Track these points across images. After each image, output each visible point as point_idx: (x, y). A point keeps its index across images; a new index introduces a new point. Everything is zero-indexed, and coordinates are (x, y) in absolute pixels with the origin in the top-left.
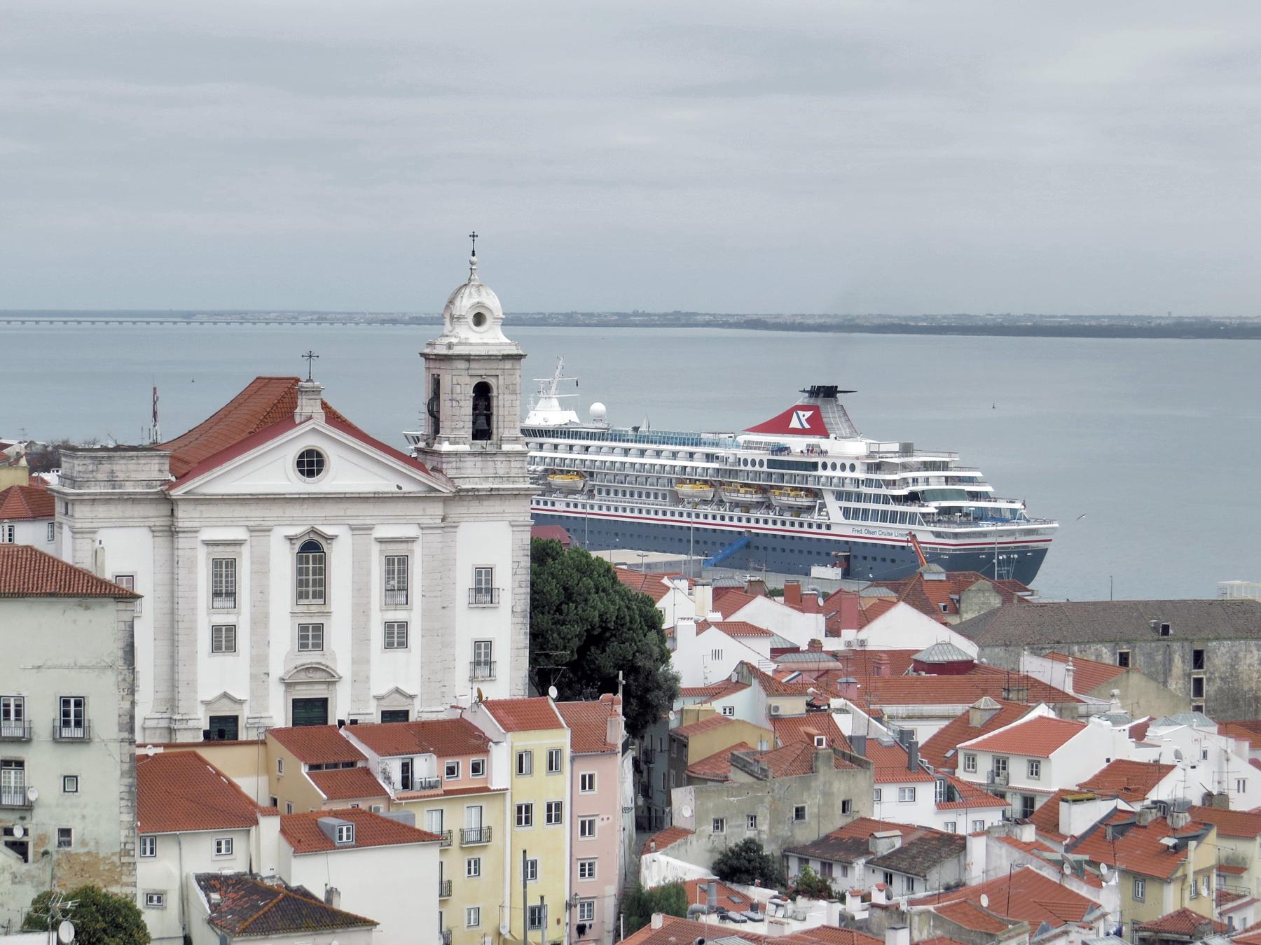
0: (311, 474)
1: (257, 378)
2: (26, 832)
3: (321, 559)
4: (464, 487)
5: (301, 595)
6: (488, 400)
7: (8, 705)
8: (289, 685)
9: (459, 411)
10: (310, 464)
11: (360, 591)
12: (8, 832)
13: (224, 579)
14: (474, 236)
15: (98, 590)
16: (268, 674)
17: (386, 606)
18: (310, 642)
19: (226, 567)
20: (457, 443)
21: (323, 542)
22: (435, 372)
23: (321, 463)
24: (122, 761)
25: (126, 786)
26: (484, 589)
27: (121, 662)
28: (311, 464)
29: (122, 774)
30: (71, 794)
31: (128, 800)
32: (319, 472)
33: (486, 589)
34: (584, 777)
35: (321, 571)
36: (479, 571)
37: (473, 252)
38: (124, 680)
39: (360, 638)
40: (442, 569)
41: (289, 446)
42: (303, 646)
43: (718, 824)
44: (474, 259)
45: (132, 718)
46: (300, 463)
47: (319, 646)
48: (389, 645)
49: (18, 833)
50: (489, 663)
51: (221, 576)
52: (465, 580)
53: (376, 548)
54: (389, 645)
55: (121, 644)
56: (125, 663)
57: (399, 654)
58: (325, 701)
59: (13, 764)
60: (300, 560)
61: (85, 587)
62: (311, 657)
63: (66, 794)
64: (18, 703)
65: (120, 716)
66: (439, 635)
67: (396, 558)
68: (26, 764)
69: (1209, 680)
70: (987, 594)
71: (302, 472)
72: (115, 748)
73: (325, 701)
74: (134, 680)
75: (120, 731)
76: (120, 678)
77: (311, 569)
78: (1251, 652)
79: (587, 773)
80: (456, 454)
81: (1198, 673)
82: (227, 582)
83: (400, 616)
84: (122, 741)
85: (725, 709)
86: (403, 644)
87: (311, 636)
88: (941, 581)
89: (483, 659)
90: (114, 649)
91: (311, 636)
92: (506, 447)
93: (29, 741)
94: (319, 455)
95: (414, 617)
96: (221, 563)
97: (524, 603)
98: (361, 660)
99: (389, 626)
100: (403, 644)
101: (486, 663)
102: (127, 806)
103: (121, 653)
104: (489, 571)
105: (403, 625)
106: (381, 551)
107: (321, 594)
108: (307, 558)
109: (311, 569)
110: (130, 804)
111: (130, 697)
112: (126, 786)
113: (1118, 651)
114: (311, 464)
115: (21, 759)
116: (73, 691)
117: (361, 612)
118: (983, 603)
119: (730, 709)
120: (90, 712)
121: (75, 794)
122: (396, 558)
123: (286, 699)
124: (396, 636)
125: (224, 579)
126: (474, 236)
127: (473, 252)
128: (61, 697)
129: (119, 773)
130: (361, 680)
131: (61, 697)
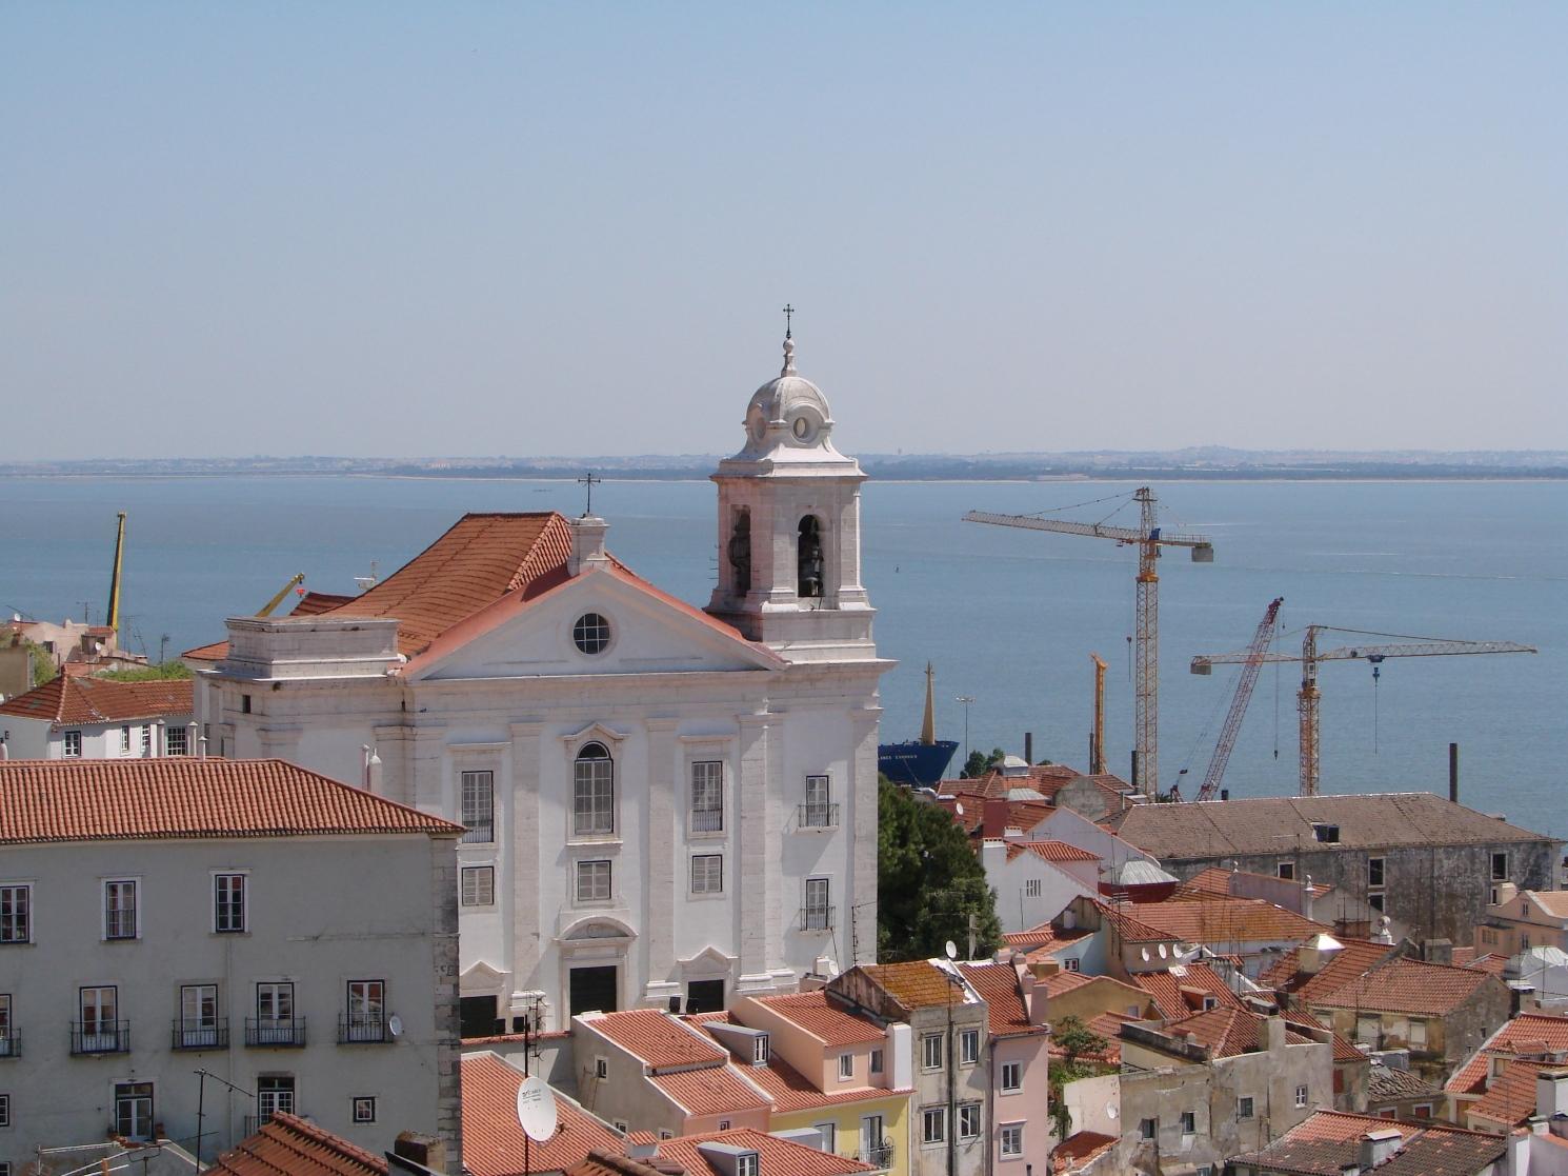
0: (592, 648)
1: (465, 517)
3: (608, 770)
4: (795, 662)
6: (816, 540)
7: (268, 996)
8: (566, 953)
9: (783, 553)
13: (477, 801)
14: (789, 310)
15: (403, 823)
16: (538, 935)
18: (594, 887)
19: (481, 784)
20: (780, 602)
21: (607, 742)
22: (740, 503)
23: (605, 633)
24: (440, 1074)
25: (447, 1109)
27: (439, 928)
28: (591, 634)
29: (442, 1095)
30: (365, 1124)
31: (450, 1130)
32: (603, 645)
33: (822, 806)
34: (1006, 1068)
37: (788, 332)
38: (444, 954)
42: (584, 894)
43: (1150, 1127)
44: (790, 341)
46: (578, 634)
47: (606, 891)
50: (825, 910)
51: (473, 798)
54: (697, 887)
55: (439, 901)
56: (444, 929)
58: (613, 970)
59: (276, 1081)
60: (580, 771)
61: (382, 819)
62: (595, 913)
63: (357, 1124)
64: (283, 992)
65: (437, 1007)
67: (707, 765)
68: (296, 1082)
69: (1389, 897)
70: (1088, 793)
71: (580, 646)
73: (613, 970)
74: (458, 953)
75: (438, 1028)
76: (439, 950)
77: (593, 782)
78: (1440, 861)
79: (1010, 1064)
80: (781, 616)
81: (1376, 890)
82: (481, 805)
84: (442, 1042)
85: (1067, 963)
87: (595, 875)
88: (1024, 778)
89: (817, 905)
91: (595, 875)
92: (845, 606)
93: (303, 1045)
94: (602, 621)
95: (728, 850)
96: (473, 777)
101: (821, 910)
102: (449, 1139)
103: (438, 914)
106: (687, 755)
108: (589, 767)
109: (593, 782)
110: (453, 1137)
111: (452, 979)
112: (447, 1109)
113: (1279, 864)
114: (591, 634)
115: (289, 1075)
116: (365, 971)
118: (1083, 806)
119: (1074, 963)
120: (394, 999)
121: (372, 1124)
122: (707, 765)
123: (561, 969)
124: (707, 875)
125: (477, 801)
126: (789, 310)
127: (788, 332)
128: (349, 982)
129: (436, 1093)
131: (349, 982)
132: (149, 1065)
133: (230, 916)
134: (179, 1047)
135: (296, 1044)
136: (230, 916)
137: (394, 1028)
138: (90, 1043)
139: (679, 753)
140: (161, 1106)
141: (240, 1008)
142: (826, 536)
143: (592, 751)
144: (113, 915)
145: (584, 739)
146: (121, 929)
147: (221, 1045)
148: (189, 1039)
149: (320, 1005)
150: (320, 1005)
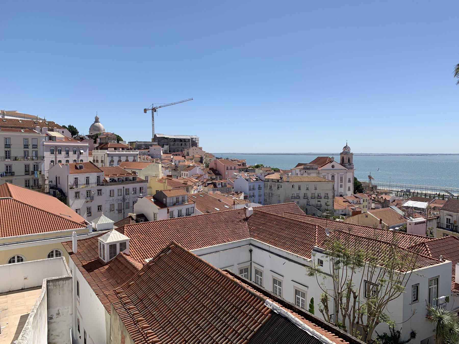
0: (333, 168)
10: (333, 167)
11: (338, 181)
17: (341, 183)
26: (349, 181)
35: (334, 179)
36: (349, 179)
39: (338, 186)
40: (345, 179)
48: (341, 187)
50: (350, 189)
52: (348, 180)
53: (339, 176)
54: (341, 187)
57: (342, 188)
60: (332, 177)
66: (345, 186)
72: (331, 199)
83: (341, 184)
86: (342, 187)
90: (331, 188)
95: (343, 184)
97: (353, 182)
98: (338, 189)
99: (341, 185)
100: (342, 187)
104: (350, 179)
105: (342, 185)
116: (327, 193)
117: (338, 183)
120: (329, 195)
124: (341, 186)
130: (338, 191)
138: (305, 198)
139: (339, 176)
141: (316, 195)
142: (350, 159)
143: (333, 176)
145: (332, 175)
147: (315, 198)
148: (312, 198)
149: (323, 195)
150: (323, 195)
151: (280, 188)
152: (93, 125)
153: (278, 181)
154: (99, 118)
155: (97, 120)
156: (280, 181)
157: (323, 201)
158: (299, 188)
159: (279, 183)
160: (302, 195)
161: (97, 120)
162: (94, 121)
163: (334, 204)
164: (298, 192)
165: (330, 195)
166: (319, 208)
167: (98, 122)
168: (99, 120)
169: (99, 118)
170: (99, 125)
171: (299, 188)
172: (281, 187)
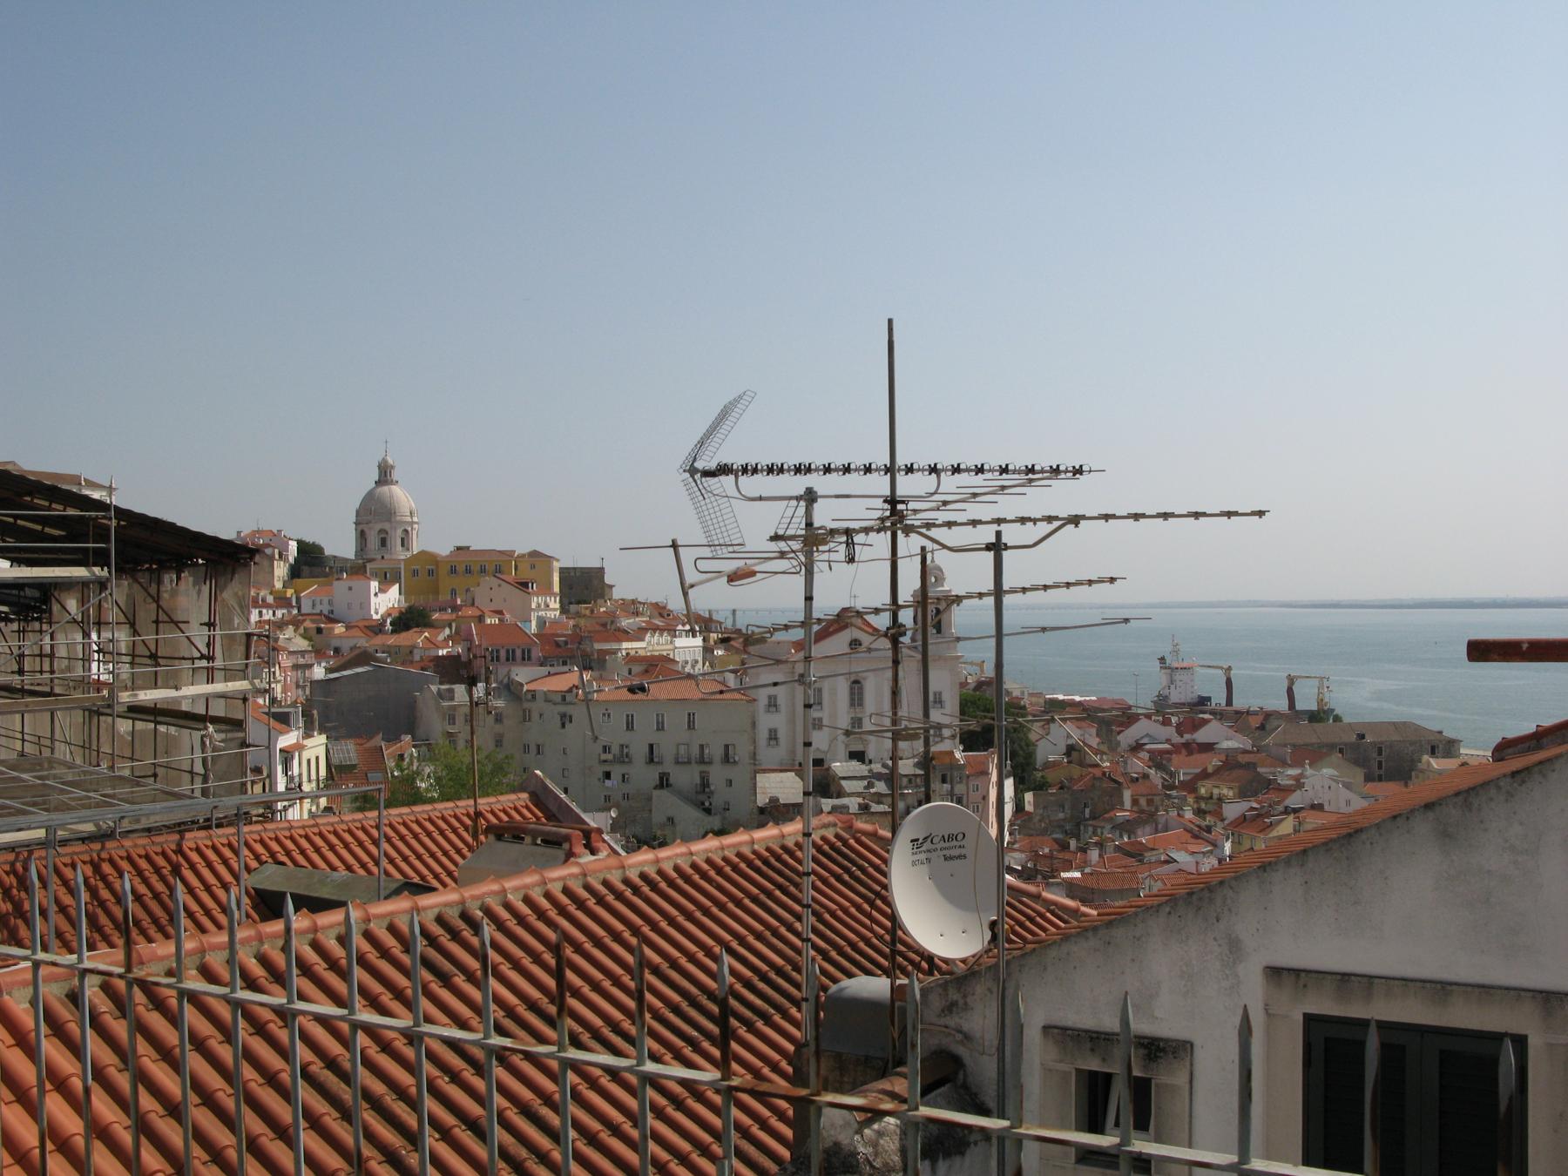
2: (710, 804)
5: (852, 704)
8: (847, 746)
10: (855, 643)
12: (703, 804)
41: (844, 637)
45: (755, 754)
49: (707, 804)
60: (852, 689)
107: (861, 704)
132: (668, 767)
133: (691, 725)
134: (677, 762)
135: (710, 763)
136: (691, 725)
137: (737, 759)
140: (671, 781)
141: (695, 751)
143: (856, 682)
144: (658, 723)
146: (660, 727)
147: (689, 762)
149: (716, 752)
150: (716, 752)
151: (568, 725)
152: (370, 496)
153: (564, 698)
154: (392, 467)
155: (385, 475)
156: (569, 697)
157: (717, 774)
158: (630, 726)
159: (562, 709)
160: (639, 751)
161: (385, 475)
162: (377, 479)
163: (755, 784)
164: (626, 737)
165: (741, 752)
166: (702, 797)
167: (392, 483)
168: (396, 475)
169: (392, 467)
170: (391, 497)
171: (630, 726)
172: (571, 721)
